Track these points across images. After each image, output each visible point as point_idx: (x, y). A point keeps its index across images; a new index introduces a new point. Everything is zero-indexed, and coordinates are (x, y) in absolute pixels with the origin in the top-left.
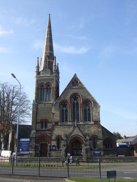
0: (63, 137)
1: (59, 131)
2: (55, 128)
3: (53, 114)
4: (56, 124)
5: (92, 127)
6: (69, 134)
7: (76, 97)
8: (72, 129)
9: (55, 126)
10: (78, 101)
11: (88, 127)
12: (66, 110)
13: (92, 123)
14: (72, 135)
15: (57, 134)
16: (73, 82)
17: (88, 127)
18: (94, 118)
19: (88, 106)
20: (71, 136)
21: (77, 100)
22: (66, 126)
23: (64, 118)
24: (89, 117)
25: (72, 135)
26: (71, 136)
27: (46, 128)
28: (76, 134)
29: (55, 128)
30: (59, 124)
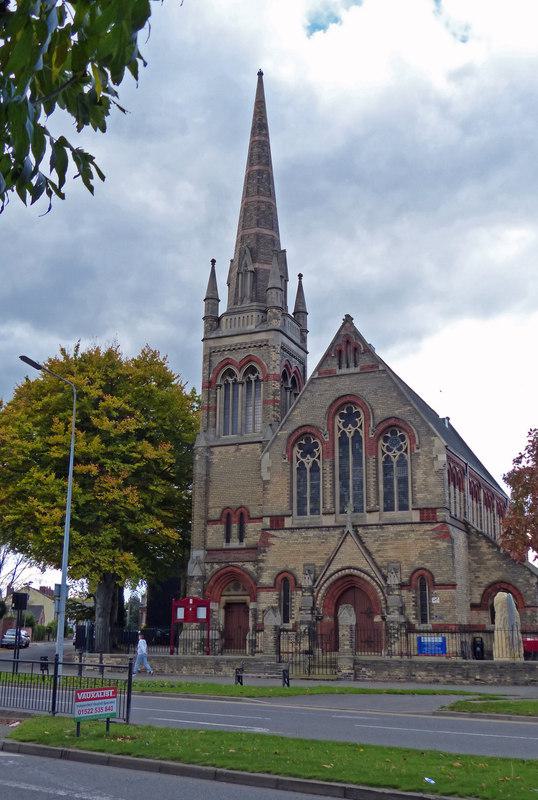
0: (299, 574)
1: (287, 553)
2: (271, 540)
3: (267, 482)
4: (277, 522)
5: (412, 535)
6: (322, 563)
7: (349, 409)
8: (333, 542)
9: (272, 532)
10: (361, 427)
11: (398, 534)
12: (315, 468)
13: (416, 516)
14: (333, 568)
15: (281, 567)
16: (340, 351)
17: (398, 534)
18: (419, 496)
19: (400, 449)
20: (328, 573)
21: (355, 425)
22: (311, 533)
23: (306, 499)
24: (404, 494)
25: (333, 568)
26: (328, 573)
27: (241, 541)
28: (348, 564)
29: (271, 540)
30: (288, 523)
